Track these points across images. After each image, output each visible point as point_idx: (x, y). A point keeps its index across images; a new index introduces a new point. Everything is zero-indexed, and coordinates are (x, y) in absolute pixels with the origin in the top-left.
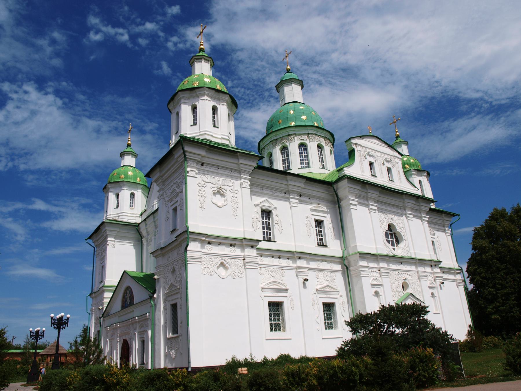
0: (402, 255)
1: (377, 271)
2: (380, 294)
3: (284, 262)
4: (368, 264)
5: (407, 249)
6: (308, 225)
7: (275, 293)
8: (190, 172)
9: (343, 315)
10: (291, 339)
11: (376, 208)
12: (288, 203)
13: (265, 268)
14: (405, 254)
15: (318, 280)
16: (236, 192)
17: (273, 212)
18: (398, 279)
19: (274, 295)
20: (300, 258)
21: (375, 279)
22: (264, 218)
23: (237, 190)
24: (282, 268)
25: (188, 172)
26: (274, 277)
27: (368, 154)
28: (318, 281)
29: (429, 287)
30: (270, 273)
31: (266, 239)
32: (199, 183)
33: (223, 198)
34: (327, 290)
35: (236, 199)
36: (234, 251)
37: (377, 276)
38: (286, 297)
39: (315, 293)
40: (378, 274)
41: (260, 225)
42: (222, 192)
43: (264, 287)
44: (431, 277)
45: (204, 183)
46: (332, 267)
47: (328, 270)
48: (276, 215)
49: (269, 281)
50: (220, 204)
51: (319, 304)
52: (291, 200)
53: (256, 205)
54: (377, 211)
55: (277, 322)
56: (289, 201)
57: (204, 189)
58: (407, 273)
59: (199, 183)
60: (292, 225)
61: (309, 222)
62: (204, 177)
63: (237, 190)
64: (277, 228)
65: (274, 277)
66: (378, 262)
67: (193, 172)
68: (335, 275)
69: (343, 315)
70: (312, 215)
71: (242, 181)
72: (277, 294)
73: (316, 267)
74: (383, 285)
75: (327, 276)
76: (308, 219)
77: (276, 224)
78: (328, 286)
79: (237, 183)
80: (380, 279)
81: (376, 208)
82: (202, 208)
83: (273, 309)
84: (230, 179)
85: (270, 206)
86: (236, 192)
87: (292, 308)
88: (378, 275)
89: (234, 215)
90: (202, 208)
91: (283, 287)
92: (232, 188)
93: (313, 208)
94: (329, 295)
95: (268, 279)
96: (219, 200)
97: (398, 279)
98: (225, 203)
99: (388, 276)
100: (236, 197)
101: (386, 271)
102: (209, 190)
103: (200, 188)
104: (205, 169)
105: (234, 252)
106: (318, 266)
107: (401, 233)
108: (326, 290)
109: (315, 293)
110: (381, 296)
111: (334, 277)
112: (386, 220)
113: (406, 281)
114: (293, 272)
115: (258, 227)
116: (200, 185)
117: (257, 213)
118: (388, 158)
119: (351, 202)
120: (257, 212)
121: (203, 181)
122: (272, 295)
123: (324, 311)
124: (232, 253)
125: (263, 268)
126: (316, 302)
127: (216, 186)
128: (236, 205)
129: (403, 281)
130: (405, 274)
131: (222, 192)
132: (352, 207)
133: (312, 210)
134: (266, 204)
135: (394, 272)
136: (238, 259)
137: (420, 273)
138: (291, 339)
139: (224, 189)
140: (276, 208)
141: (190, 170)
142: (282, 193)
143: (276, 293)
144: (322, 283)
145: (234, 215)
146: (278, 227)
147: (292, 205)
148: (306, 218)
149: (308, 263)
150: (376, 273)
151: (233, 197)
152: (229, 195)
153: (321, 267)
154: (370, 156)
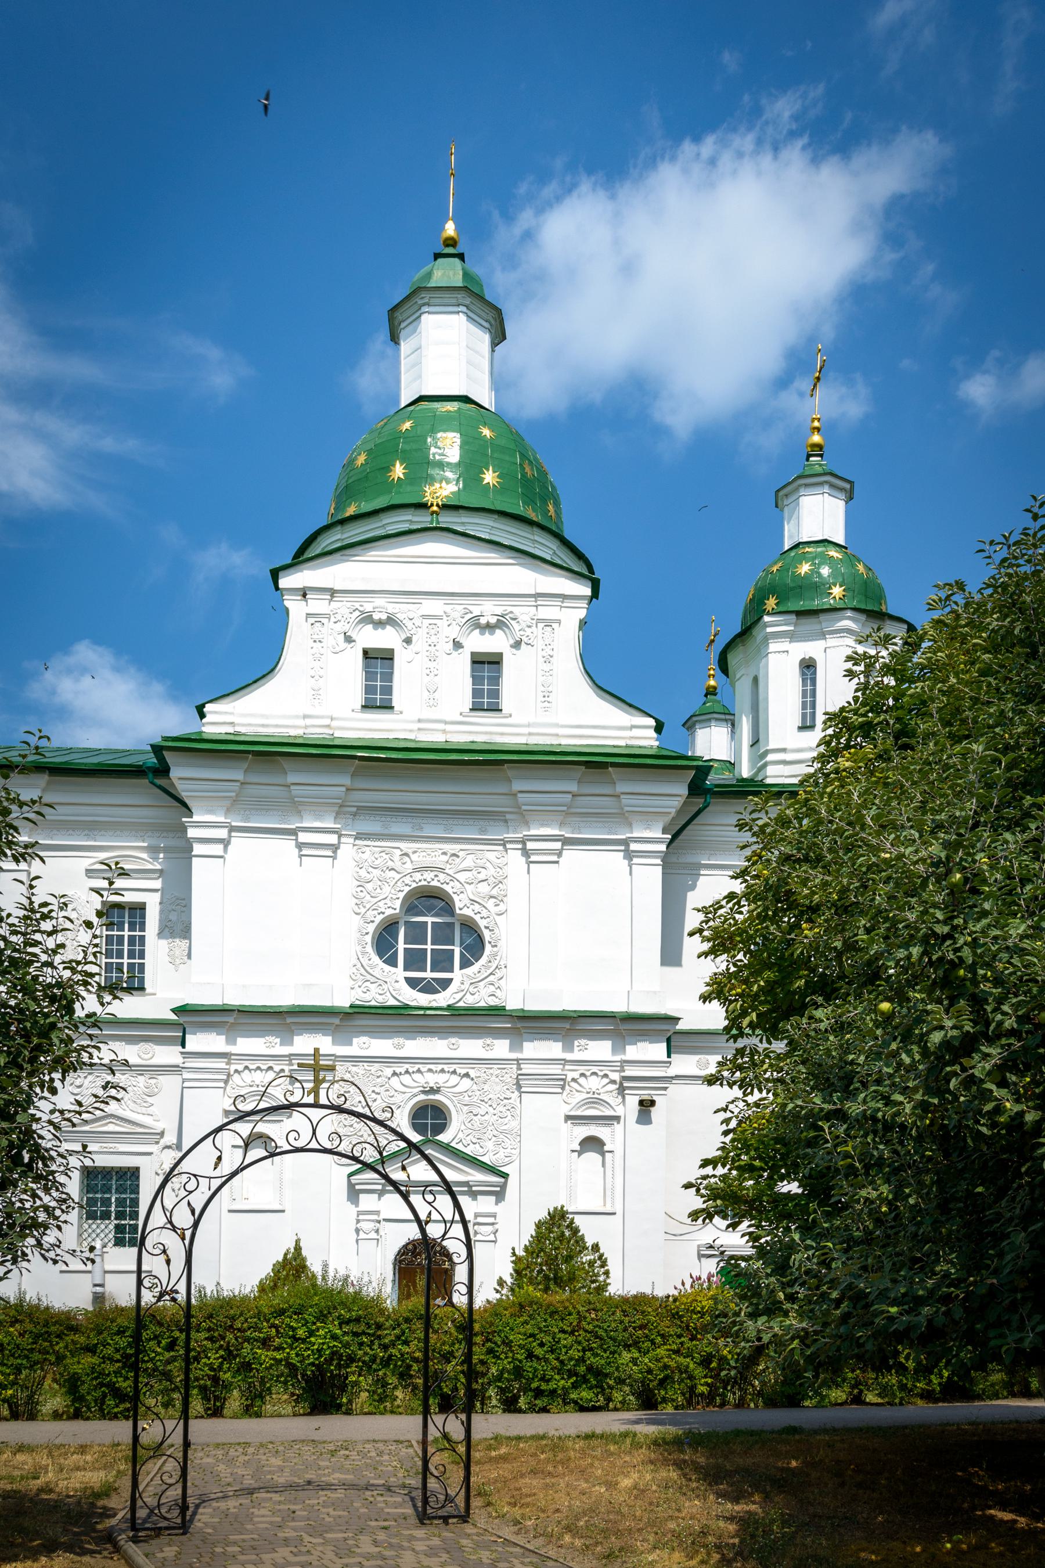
0: (451, 1002)
5: (492, 978)
14: (481, 998)
18: (393, 1093)
27: (367, 619)
29: (568, 1118)
34: (111, 1128)
44: (607, 1080)
46: (146, 1057)
54: (347, 849)
58: (452, 1068)
68: (153, 1081)
94: (111, 1145)
97: (393, 1093)
107: (477, 918)
113: (437, 1097)
118: (489, 611)
129: (422, 1097)
130: (442, 1071)
137: (527, 1069)
154: (379, 624)
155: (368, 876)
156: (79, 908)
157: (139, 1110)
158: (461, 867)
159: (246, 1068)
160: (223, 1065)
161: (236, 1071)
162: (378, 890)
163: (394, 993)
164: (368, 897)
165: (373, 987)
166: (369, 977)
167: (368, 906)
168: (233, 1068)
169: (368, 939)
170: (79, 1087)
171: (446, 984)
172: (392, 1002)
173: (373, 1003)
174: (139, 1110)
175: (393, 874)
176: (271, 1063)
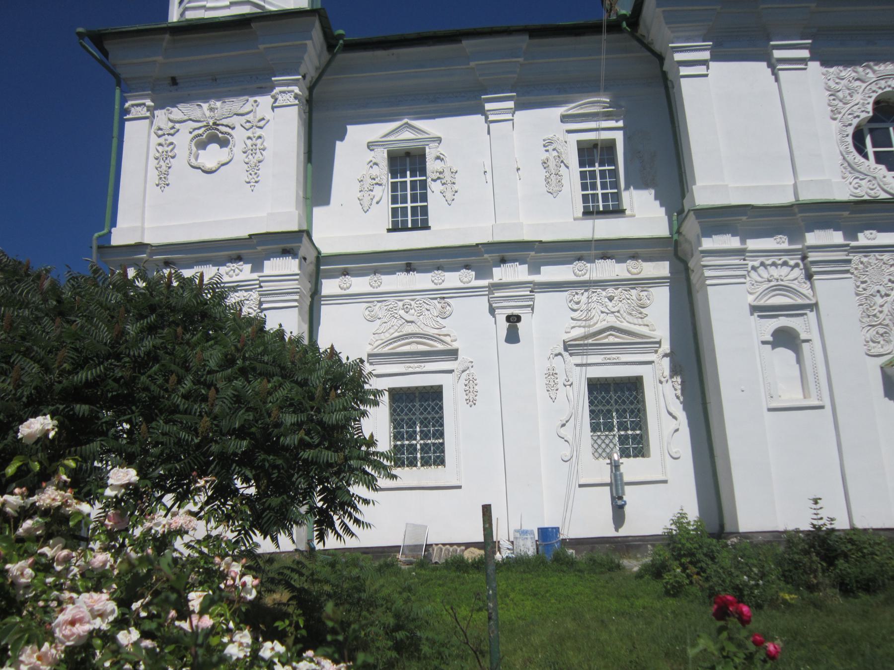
1: (792, 263)
2: (803, 336)
3: (452, 279)
4: (743, 241)
6: (552, 164)
7: (412, 365)
8: (133, 110)
9: (670, 414)
10: (460, 487)
11: (805, 54)
12: (480, 118)
13: (384, 304)
15: (575, 315)
16: (261, 124)
17: (427, 150)
19: (410, 370)
20: (503, 261)
21: (782, 289)
22: (408, 173)
23: (263, 119)
24: (442, 295)
25: (127, 112)
26: (412, 322)
28: (573, 319)
30: (402, 312)
31: (410, 226)
32: (160, 129)
33: (226, 150)
34: (612, 339)
35: (259, 141)
36: (237, 271)
37: (791, 276)
38: (451, 371)
39: (560, 354)
40: (796, 270)
41: (384, 193)
42: (220, 135)
43: (376, 351)
45: (171, 124)
47: (617, 283)
48: (438, 158)
49: (396, 334)
50: (210, 165)
51: (570, 385)
52: (488, 106)
53: (371, 146)
54: (814, 66)
55: (407, 442)
56: (481, 111)
57: (171, 139)
59: (160, 129)
60: (489, 175)
61: (555, 154)
62: (174, 110)
63: (263, 119)
64: (437, 192)
65: (412, 322)
66: (795, 235)
67: (139, 109)
68: (645, 293)
69: (670, 414)
70: (569, 132)
71: (277, 89)
73: (572, 278)
74: (816, 304)
75: (611, 299)
76: (550, 148)
77: (433, 180)
78: (612, 328)
79: (265, 101)
80: (805, 288)
81: (805, 54)
82: (163, 181)
83: (421, 406)
84: (246, 97)
85: (420, 136)
86: (261, 124)
87: (471, 402)
88: (798, 273)
89: (249, 182)
90: (163, 181)
91: (440, 347)
92: (250, 117)
93: (570, 112)
94: (614, 356)
95: (392, 331)
96: (212, 155)
98: (225, 159)
99: (847, 272)
100: (260, 137)
101: (841, 256)
102: (183, 139)
103: (161, 140)
105: (237, 275)
106: (575, 274)
108: (606, 341)
109: (560, 354)
110: (805, 346)
111: (645, 301)
112: (864, 85)
114: (483, 303)
116: (160, 132)
117: (376, 164)
119: (678, 57)
120: (374, 161)
121: (172, 121)
122: (403, 370)
123: (591, 403)
124: (231, 277)
125: (378, 302)
126: (561, 379)
127: (205, 123)
128: (259, 155)
131: (220, 135)
132: (684, 71)
133: (565, 118)
134: (407, 135)
136: (246, 290)
138: (460, 487)
139: (227, 126)
140: (439, 140)
141: (133, 106)
143: (416, 365)
144: (592, 322)
145: (249, 182)
146: (442, 188)
147: (491, 118)
149: (535, 269)
150: (786, 270)
151: (249, 138)
152: (239, 136)
153: (596, 276)
155: (837, 87)
156: (559, 147)
157: (636, 321)
159: (762, 264)
160: (742, 262)
161: (754, 268)
162: (849, 98)
163: (885, 187)
164: (841, 104)
165: (863, 183)
166: (857, 175)
167: (843, 111)
168: (751, 264)
169: (850, 140)
170: (578, 303)
172: (884, 196)
173: (866, 198)
174: (636, 321)
175: (858, 83)
176: (785, 258)
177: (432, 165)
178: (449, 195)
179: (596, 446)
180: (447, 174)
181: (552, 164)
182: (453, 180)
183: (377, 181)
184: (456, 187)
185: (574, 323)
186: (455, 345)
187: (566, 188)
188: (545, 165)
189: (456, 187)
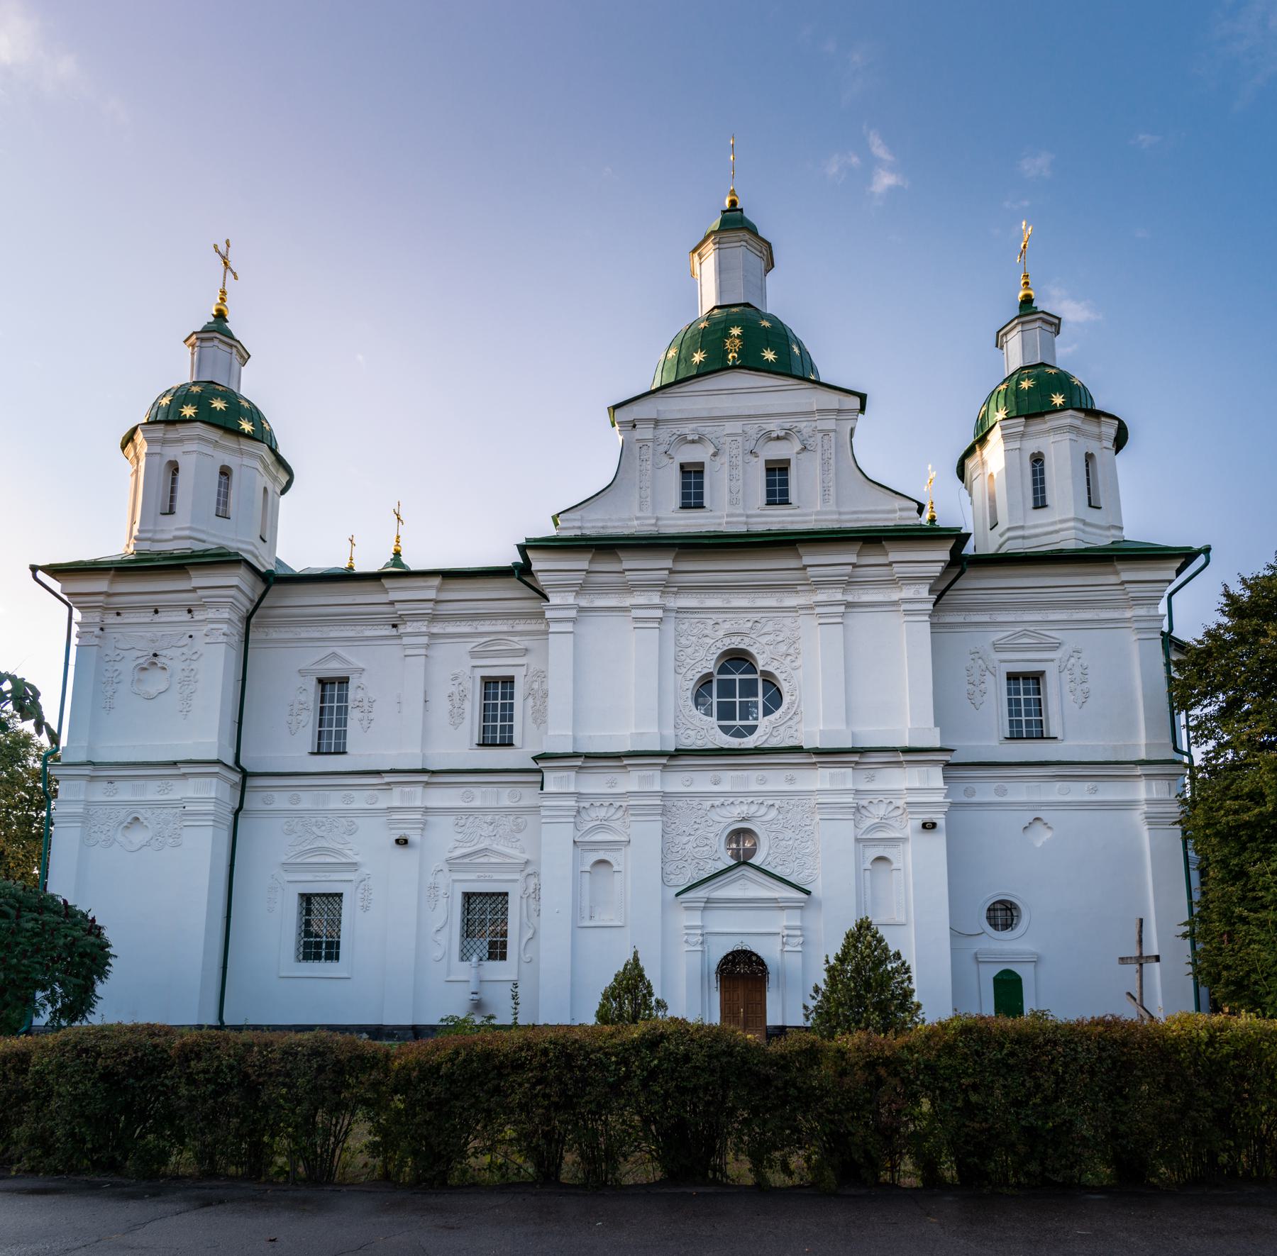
5: (790, 723)
6: (456, 697)
43: (289, 861)
72: (325, 876)
85: (346, 666)
94: (487, 874)
95: (304, 844)
104: (126, 621)
107: (776, 673)
115: (303, 724)
120: (304, 687)
135: (695, 802)
142: (386, 627)
148: (452, 680)
158: (762, 632)
171: (752, 730)
177: (353, 694)
178: (365, 723)
179: (465, 951)
180: (366, 704)
181: (456, 697)
182: (370, 709)
183: (305, 706)
184: (372, 716)
185: (457, 844)
186: (357, 859)
187: (467, 722)
188: (451, 699)
189: (372, 716)
